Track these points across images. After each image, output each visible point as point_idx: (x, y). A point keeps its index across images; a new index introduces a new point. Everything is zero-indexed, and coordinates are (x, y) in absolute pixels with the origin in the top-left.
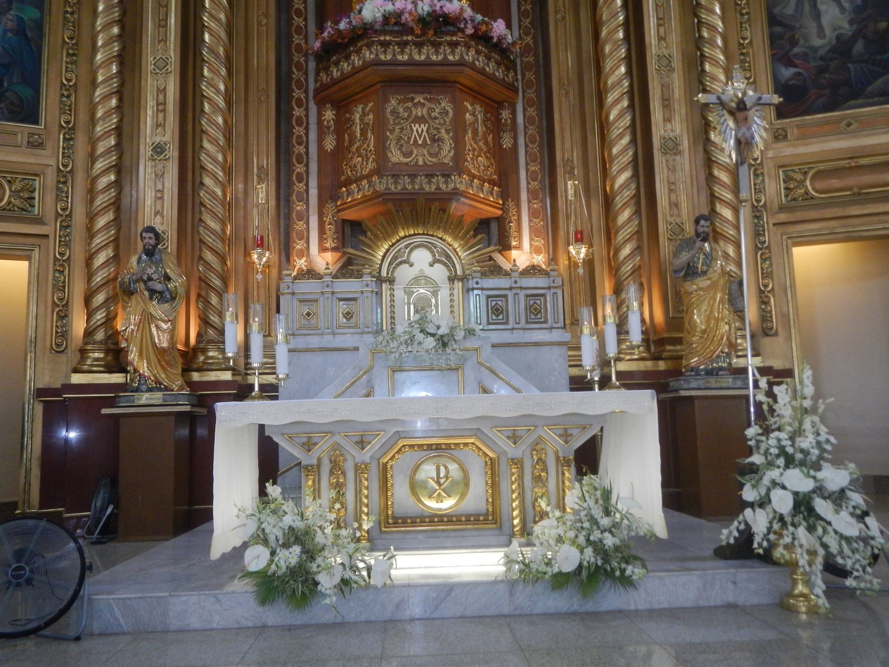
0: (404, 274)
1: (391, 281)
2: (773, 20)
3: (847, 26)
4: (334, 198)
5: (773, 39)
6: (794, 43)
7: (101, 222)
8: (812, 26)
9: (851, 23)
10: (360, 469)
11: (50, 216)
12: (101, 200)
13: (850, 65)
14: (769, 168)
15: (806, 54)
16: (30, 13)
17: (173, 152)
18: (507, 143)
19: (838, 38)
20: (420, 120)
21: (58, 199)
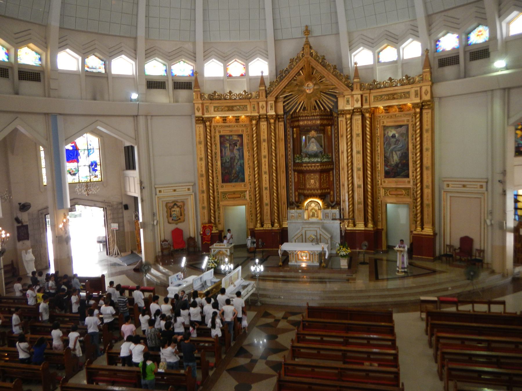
0: (310, 208)
1: (307, 210)
2: (385, 157)
3: (398, 160)
4: (297, 191)
5: (385, 160)
6: (388, 162)
7: (258, 202)
8: (392, 160)
9: (399, 160)
10: (295, 254)
11: (248, 200)
12: (258, 198)
13: (398, 169)
14: (382, 189)
15: (390, 166)
16: (242, 161)
17: (268, 189)
18: (331, 179)
19: (396, 162)
20: (312, 179)
21: (250, 196)
